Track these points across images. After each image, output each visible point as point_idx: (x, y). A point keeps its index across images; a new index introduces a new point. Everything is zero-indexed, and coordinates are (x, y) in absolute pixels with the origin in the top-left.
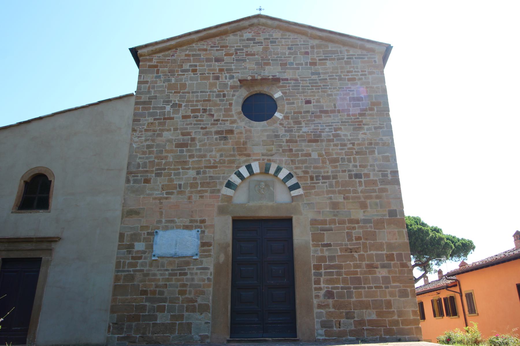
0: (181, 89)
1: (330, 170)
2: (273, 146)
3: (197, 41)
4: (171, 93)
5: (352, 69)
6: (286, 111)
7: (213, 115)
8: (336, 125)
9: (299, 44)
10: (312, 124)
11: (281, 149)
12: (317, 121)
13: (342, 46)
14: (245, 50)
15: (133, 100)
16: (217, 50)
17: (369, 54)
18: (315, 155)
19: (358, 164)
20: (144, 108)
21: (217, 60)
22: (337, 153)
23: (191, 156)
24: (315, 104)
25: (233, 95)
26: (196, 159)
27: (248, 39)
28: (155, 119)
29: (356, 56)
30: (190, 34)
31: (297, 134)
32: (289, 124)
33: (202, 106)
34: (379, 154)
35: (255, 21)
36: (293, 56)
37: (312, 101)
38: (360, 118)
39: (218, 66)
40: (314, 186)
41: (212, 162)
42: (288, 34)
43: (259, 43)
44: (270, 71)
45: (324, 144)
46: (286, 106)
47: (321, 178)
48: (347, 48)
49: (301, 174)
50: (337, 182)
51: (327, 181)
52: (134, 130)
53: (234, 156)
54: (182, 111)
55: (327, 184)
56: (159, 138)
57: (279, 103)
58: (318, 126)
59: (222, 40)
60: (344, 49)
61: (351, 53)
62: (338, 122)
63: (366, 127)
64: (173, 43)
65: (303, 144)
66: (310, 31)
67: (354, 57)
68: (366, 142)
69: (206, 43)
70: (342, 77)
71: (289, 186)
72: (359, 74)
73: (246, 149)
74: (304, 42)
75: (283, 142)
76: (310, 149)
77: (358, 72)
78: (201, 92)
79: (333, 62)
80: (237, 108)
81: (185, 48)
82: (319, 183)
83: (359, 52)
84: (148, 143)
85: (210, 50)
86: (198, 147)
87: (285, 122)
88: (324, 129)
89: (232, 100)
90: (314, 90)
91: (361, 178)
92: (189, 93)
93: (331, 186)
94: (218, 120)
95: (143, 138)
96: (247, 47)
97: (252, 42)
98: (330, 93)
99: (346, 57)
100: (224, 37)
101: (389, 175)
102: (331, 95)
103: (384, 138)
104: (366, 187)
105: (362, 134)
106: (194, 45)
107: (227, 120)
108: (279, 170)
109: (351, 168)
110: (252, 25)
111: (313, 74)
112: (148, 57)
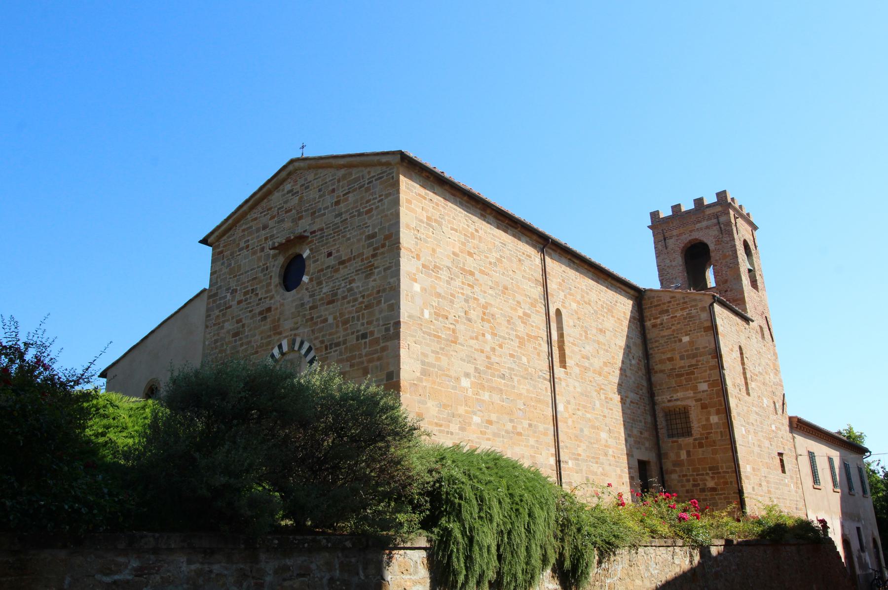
0: (238, 272)
1: (342, 333)
2: (299, 318)
3: (249, 212)
4: (231, 278)
5: (371, 197)
6: (311, 271)
7: (257, 295)
8: (351, 277)
9: (328, 180)
10: (331, 281)
11: (304, 320)
12: (337, 275)
13: (364, 169)
14: (285, 206)
15: (206, 294)
16: (265, 215)
17: (388, 169)
18: (331, 320)
19: (365, 321)
20: (214, 302)
21: (265, 227)
22: (350, 313)
23: (242, 345)
24: (336, 255)
25: (274, 266)
26: (245, 347)
27: (289, 192)
28: (220, 311)
29: (377, 177)
30: (241, 207)
31: (318, 297)
32: (313, 287)
33: (251, 286)
34: (384, 303)
35: (291, 168)
36: (321, 199)
37: (333, 251)
38: (372, 260)
39: (265, 234)
40: (327, 357)
41: (255, 346)
42: (320, 171)
43: (296, 193)
44: (304, 226)
45: (339, 303)
46: (312, 265)
47: (333, 346)
48: (368, 169)
49: (318, 345)
50: (346, 348)
51: (338, 348)
52: (207, 327)
53: (270, 336)
54: (239, 296)
55: (338, 352)
56: (222, 331)
57: (307, 263)
58: (336, 282)
59: (269, 201)
60: (365, 171)
61: (372, 174)
62: (353, 272)
63: (376, 271)
64: (230, 221)
65: (322, 308)
66: (333, 161)
67: (374, 179)
68: (375, 291)
69: (256, 211)
70: (361, 210)
71: (308, 361)
72: (376, 201)
73: (279, 326)
74: (333, 176)
75: (306, 310)
76: (327, 313)
77: (376, 198)
78: (252, 270)
79: (355, 193)
80: (276, 280)
81: (242, 222)
82: (331, 352)
83: (379, 169)
84: (215, 338)
85: (260, 217)
86: (246, 334)
87: (310, 286)
88: (340, 285)
89: (271, 272)
90: (336, 237)
91: (366, 338)
92: (242, 274)
93: (341, 354)
94: (260, 299)
95: (212, 334)
96: (286, 202)
97: (291, 194)
98: (348, 236)
99: (367, 182)
100: (270, 197)
101: (392, 329)
102: (349, 239)
103: (392, 280)
104: (369, 348)
105: (373, 281)
106: (248, 216)
107: (267, 297)
108: (302, 343)
109: (359, 328)
110: (289, 174)
111: (336, 216)
112: (217, 244)
